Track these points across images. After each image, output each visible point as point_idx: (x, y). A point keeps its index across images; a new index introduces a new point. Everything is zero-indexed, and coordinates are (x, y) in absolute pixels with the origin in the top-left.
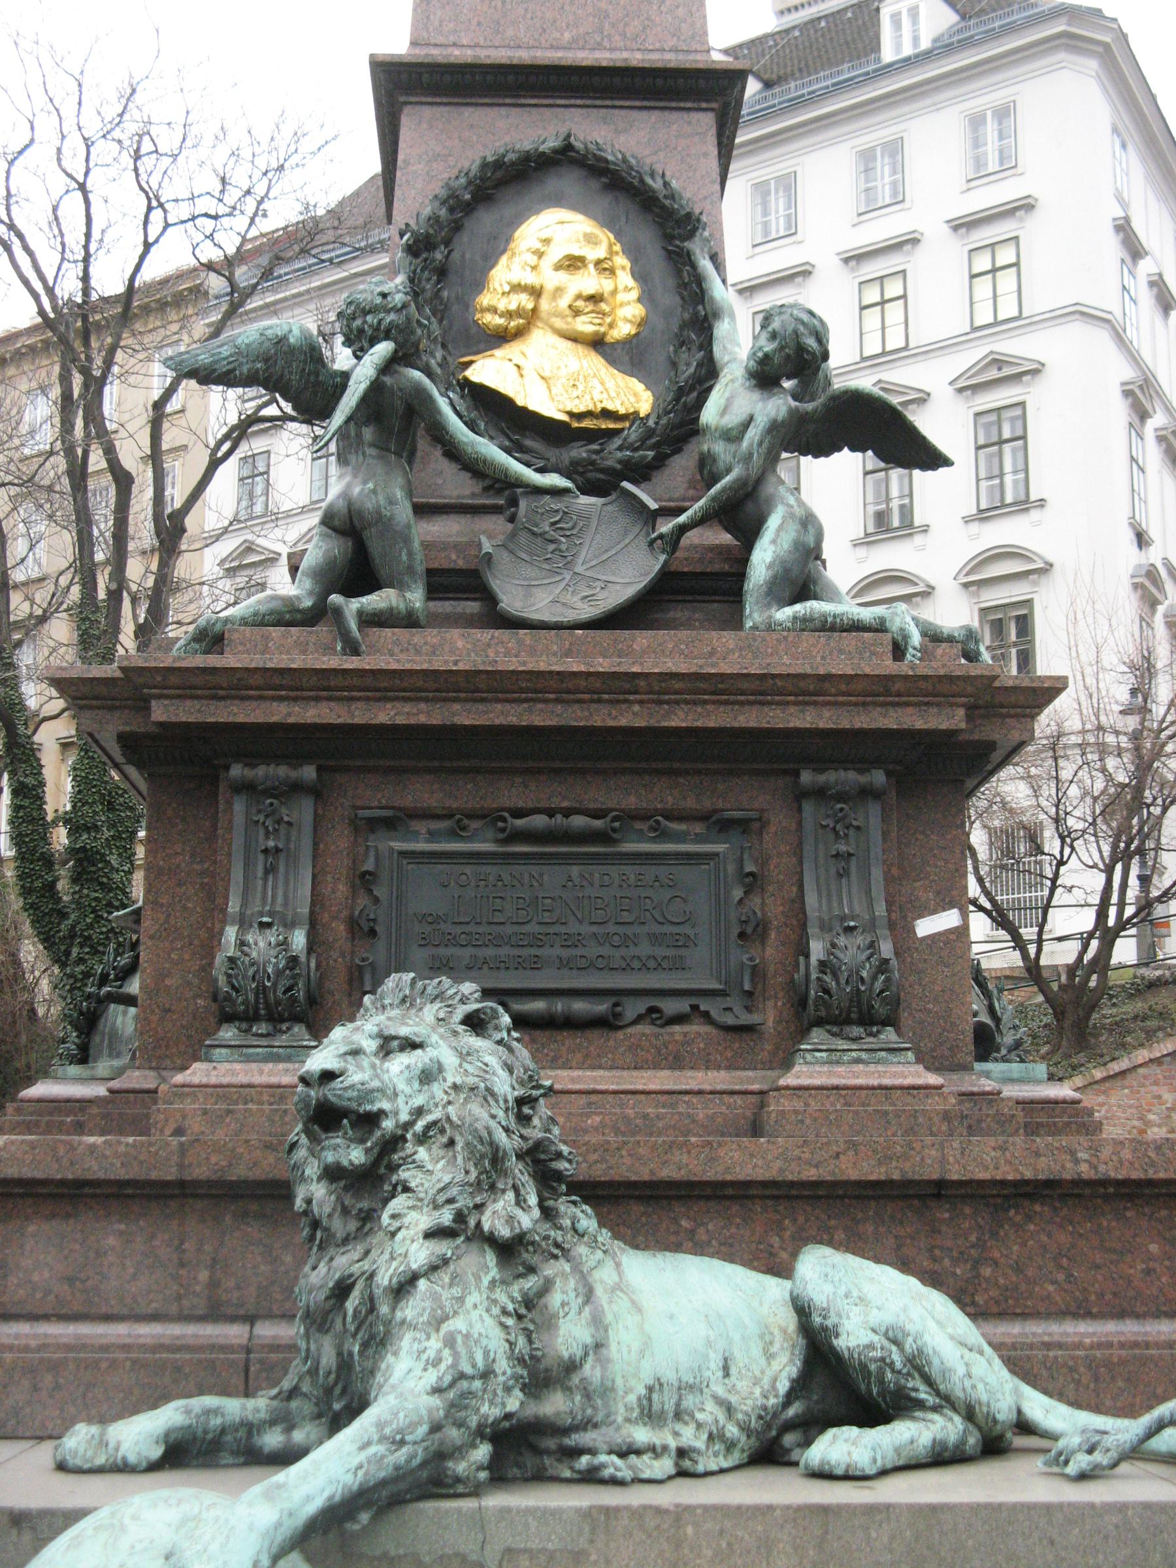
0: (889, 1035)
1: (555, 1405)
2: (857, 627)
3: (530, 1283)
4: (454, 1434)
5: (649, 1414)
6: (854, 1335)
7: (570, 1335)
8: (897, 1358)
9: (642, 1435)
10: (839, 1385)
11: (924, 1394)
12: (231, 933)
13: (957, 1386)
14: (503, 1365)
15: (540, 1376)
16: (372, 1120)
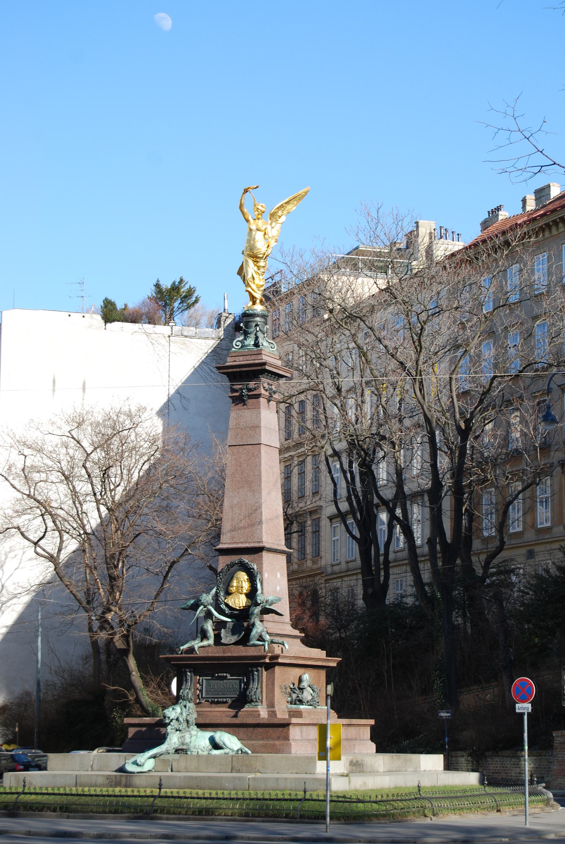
0: (256, 704)
1: (185, 747)
2: (260, 645)
3: (183, 735)
4: (169, 749)
5: (195, 748)
6: (217, 740)
7: (187, 740)
8: (221, 743)
9: (194, 750)
10: (216, 746)
11: (224, 747)
12: (181, 691)
13: (230, 747)
14: (177, 743)
15: (183, 744)
16: (169, 718)
